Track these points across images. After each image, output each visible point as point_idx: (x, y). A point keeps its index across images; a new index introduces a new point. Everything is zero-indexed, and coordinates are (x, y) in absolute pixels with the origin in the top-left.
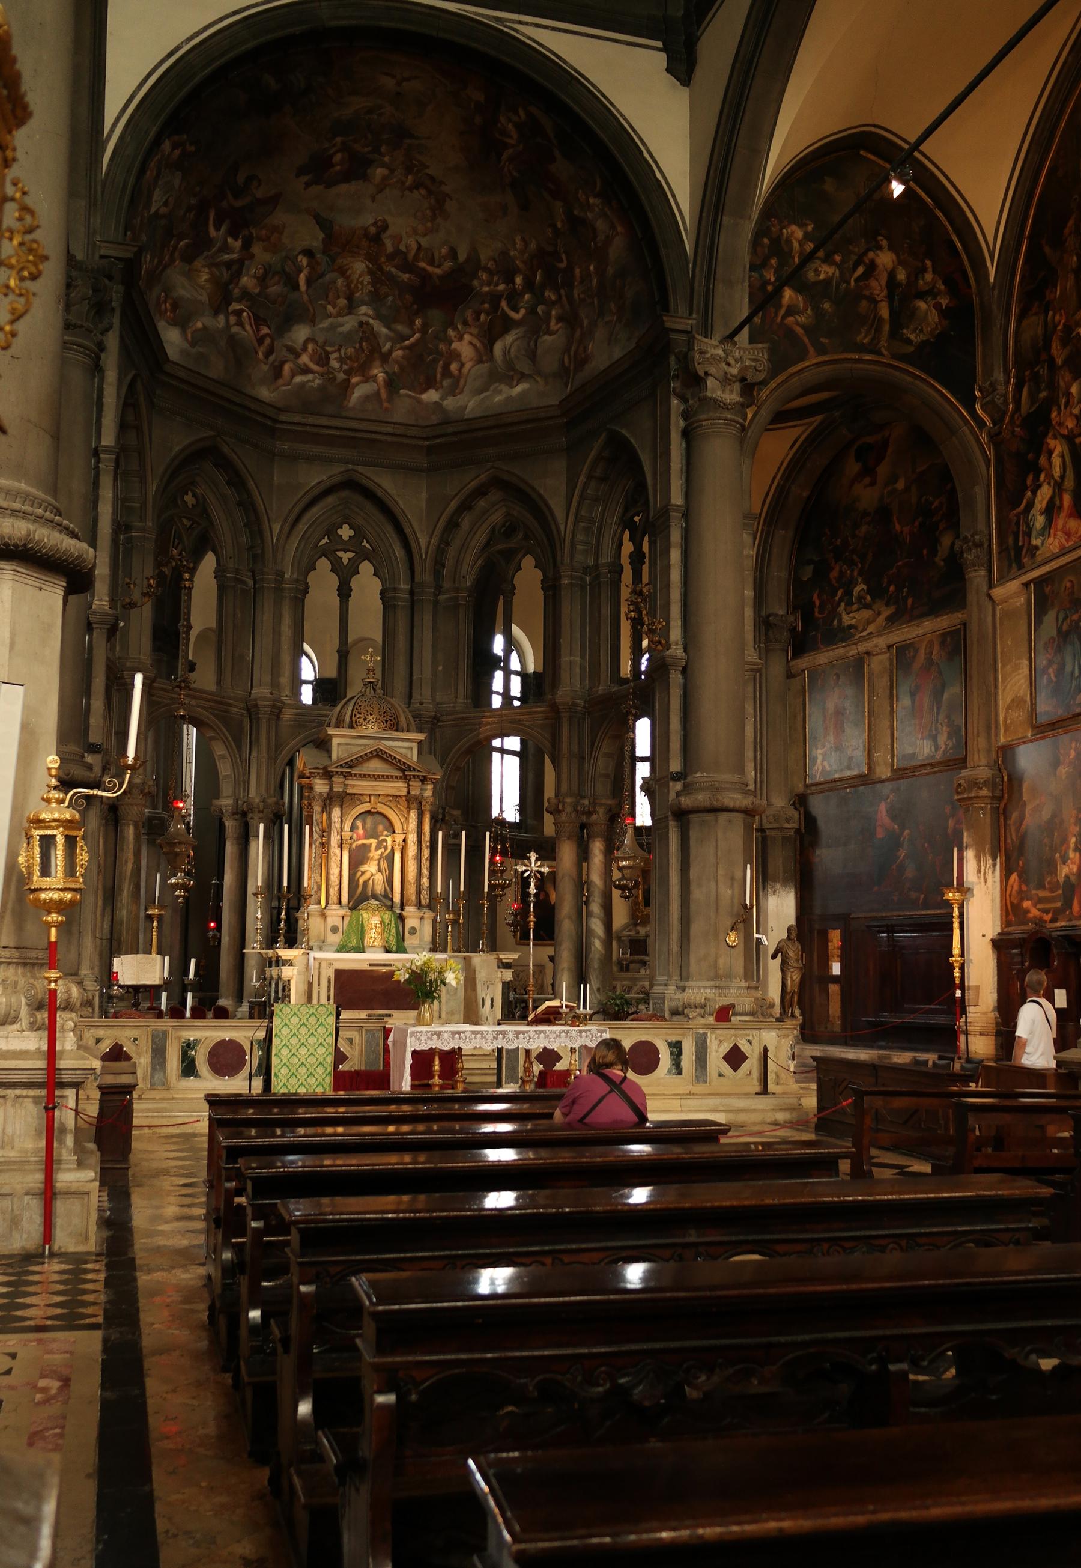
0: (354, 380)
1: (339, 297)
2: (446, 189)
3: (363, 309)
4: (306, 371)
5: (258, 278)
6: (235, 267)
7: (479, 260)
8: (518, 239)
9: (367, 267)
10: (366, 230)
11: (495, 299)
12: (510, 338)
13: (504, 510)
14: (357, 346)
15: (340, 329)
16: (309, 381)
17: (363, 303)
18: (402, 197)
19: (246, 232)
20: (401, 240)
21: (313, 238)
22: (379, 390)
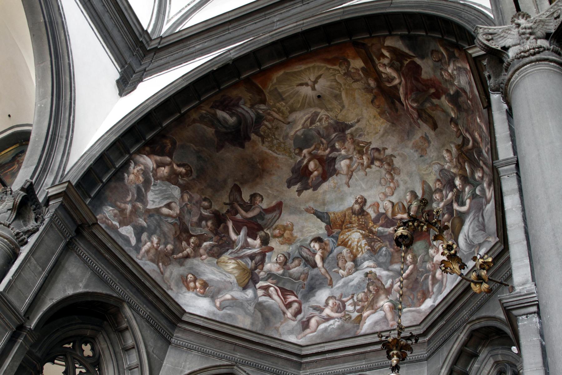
0: (365, 314)
1: (346, 262)
2: (389, 152)
3: (366, 264)
4: (329, 318)
5: (280, 264)
6: (258, 258)
7: (429, 187)
8: (446, 155)
9: (361, 234)
10: (352, 208)
11: (449, 207)
12: (466, 228)
13: (492, 361)
14: (366, 290)
15: (351, 284)
16: (331, 325)
17: (365, 260)
18: (366, 175)
19: (262, 233)
20: (378, 205)
21: (318, 228)
22: (385, 315)
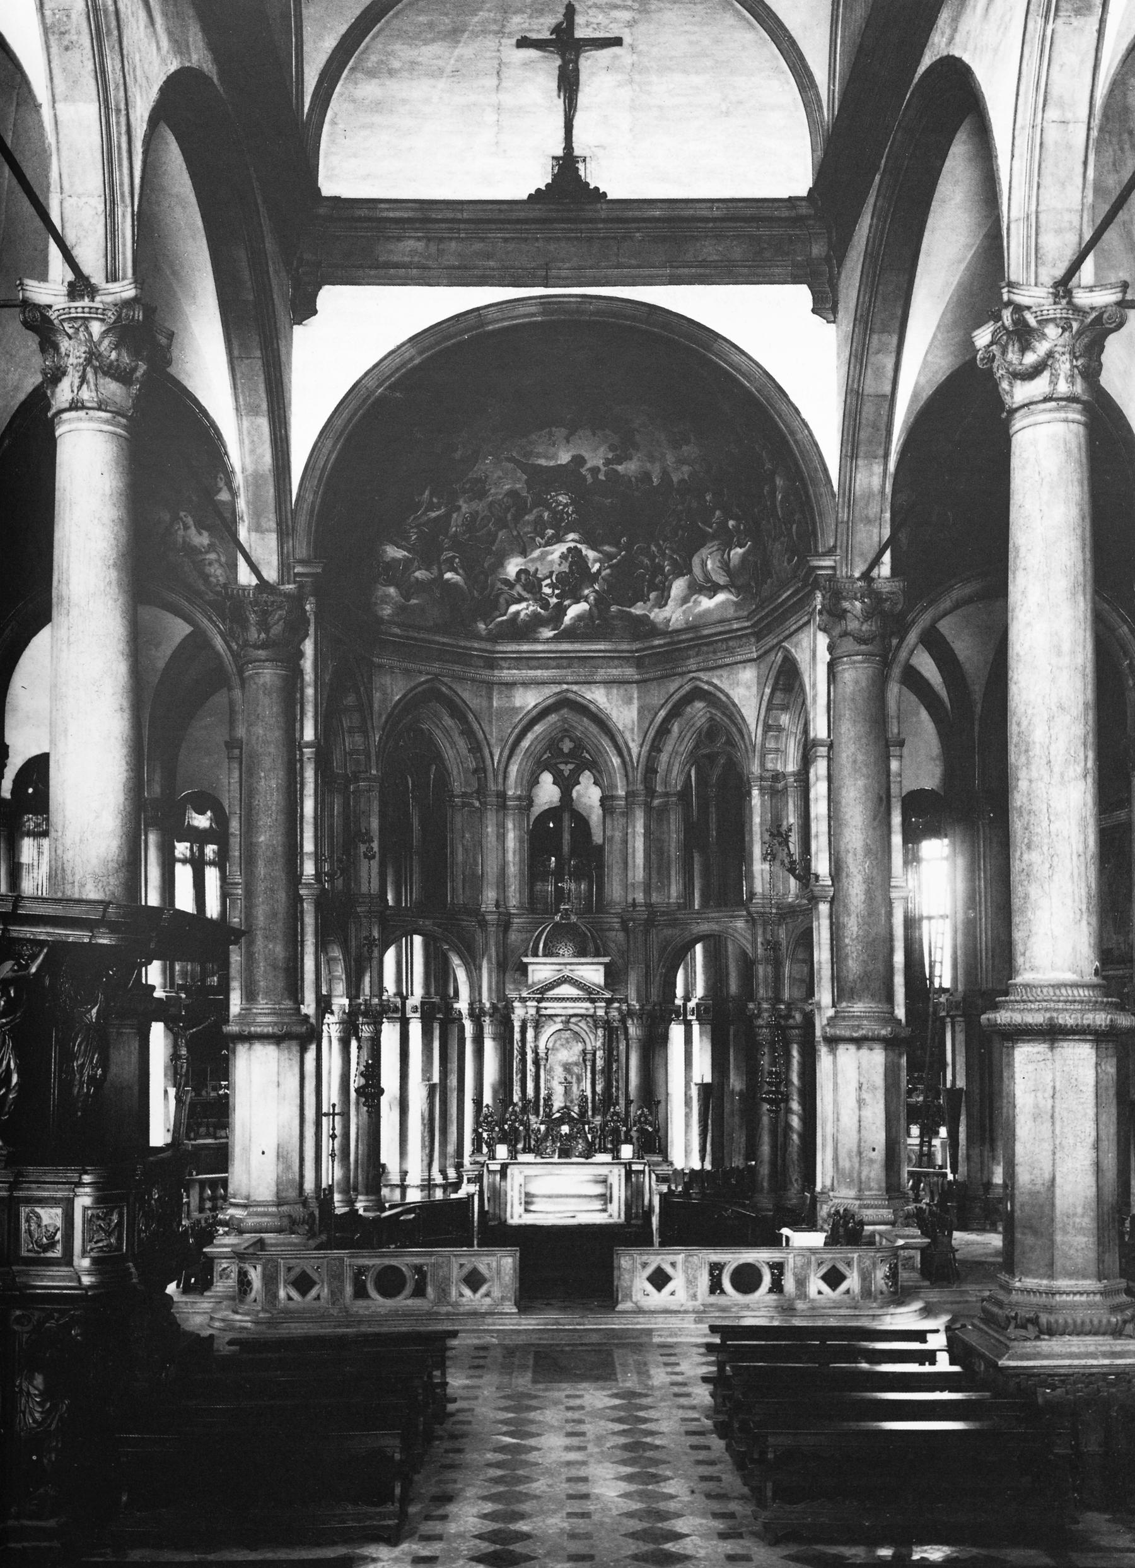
0: (566, 603)
3: (571, 536)
